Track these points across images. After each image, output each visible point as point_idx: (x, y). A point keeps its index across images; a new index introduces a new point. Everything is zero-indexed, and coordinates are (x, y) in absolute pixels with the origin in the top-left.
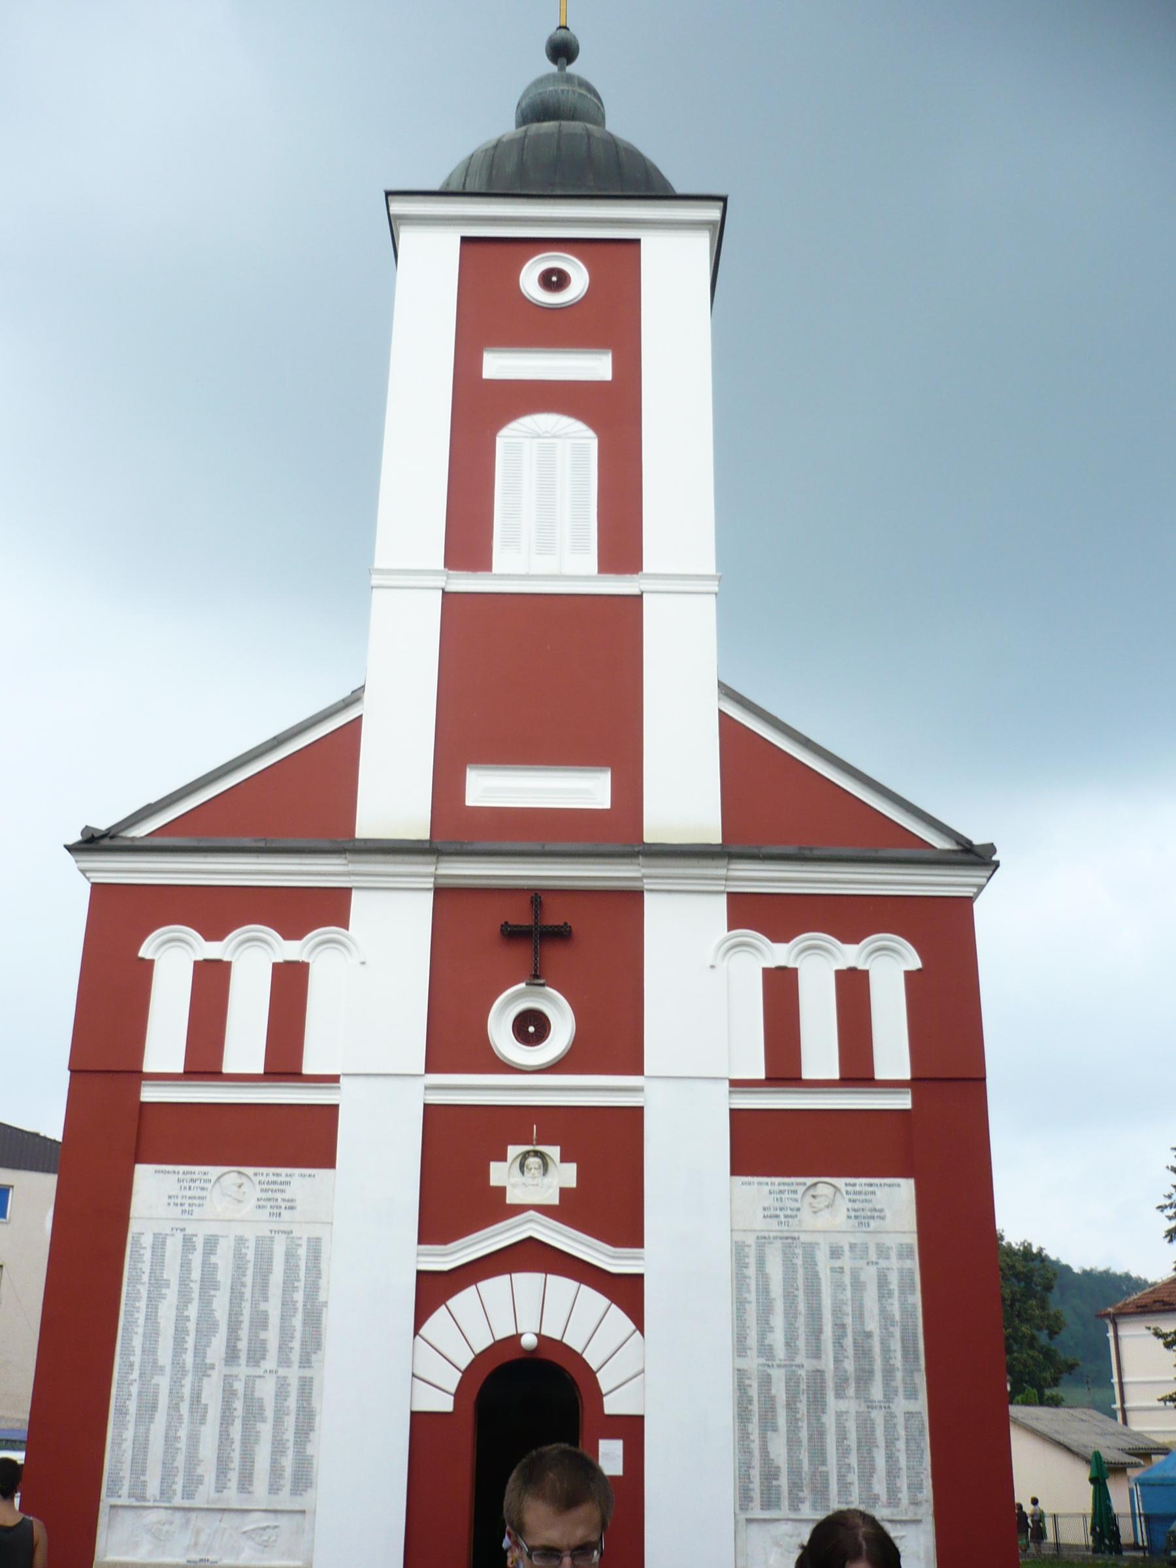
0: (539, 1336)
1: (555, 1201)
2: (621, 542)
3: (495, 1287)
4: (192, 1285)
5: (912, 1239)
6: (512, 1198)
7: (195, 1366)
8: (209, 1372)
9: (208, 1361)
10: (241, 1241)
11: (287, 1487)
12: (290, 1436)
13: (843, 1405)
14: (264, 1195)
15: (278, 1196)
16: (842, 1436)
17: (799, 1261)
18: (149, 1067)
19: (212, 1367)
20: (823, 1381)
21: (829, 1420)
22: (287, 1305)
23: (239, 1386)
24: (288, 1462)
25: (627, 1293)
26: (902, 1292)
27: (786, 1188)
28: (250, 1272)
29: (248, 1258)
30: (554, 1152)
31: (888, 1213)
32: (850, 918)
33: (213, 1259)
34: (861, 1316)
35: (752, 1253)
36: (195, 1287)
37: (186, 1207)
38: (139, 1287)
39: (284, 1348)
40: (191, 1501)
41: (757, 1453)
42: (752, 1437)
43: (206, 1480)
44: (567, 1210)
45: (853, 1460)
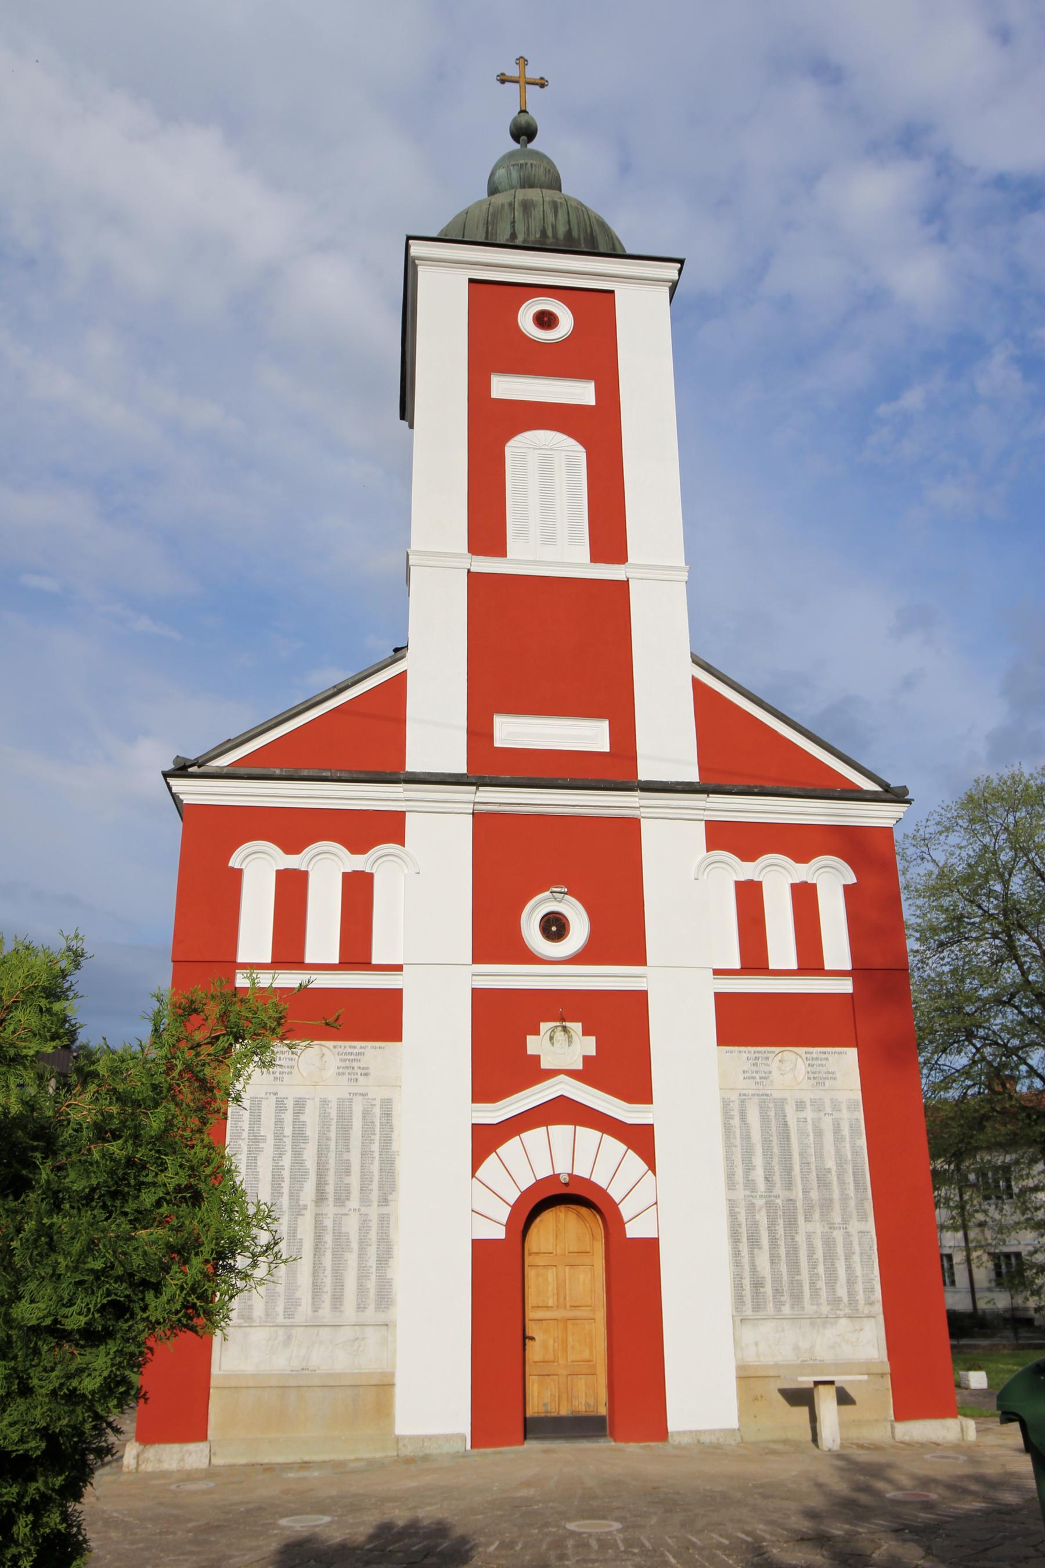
1: (579, 1066)
2: (608, 536)
3: (535, 1137)
4: (285, 1139)
5: (858, 1096)
6: (544, 1065)
7: (291, 1207)
8: (303, 1212)
9: (301, 1203)
10: (324, 1102)
11: (372, 1306)
12: (372, 1262)
13: (810, 1227)
14: (343, 1064)
15: (355, 1064)
16: (811, 1253)
17: (772, 1114)
18: (241, 959)
19: (305, 1207)
20: (795, 1208)
21: (801, 1239)
22: (365, 1154)
23: (328, 1223)
24: (372, 1284)
25: (640, 1140)
26: (852, 1137)
28: (333, 1128)
29: (331, 1116)
30: (576, 1027)
31: (838, 1075)
32: (800, 843)
33: (302, 1118)
34: (822, 1156)
35: (736, 1107)
36: (288, 1141)
37: (278, 1075)
38: (240, 1142)
39: (364, 1189)
40: (292, 1320)
41: (747, 1267)
42: (742, 1254)
43: (303, 1302)
44: (589, 1073)
45: (821, 1269)
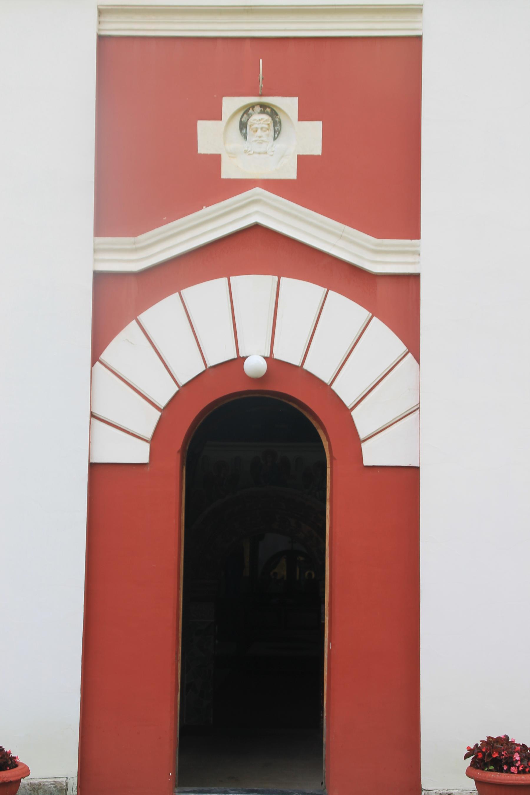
0: (270, 360)
1: (292, 174)
3: (207, 296)
6: (229, 171)
25: (396, 301)
30: (288, 105)
44: (308, 185)
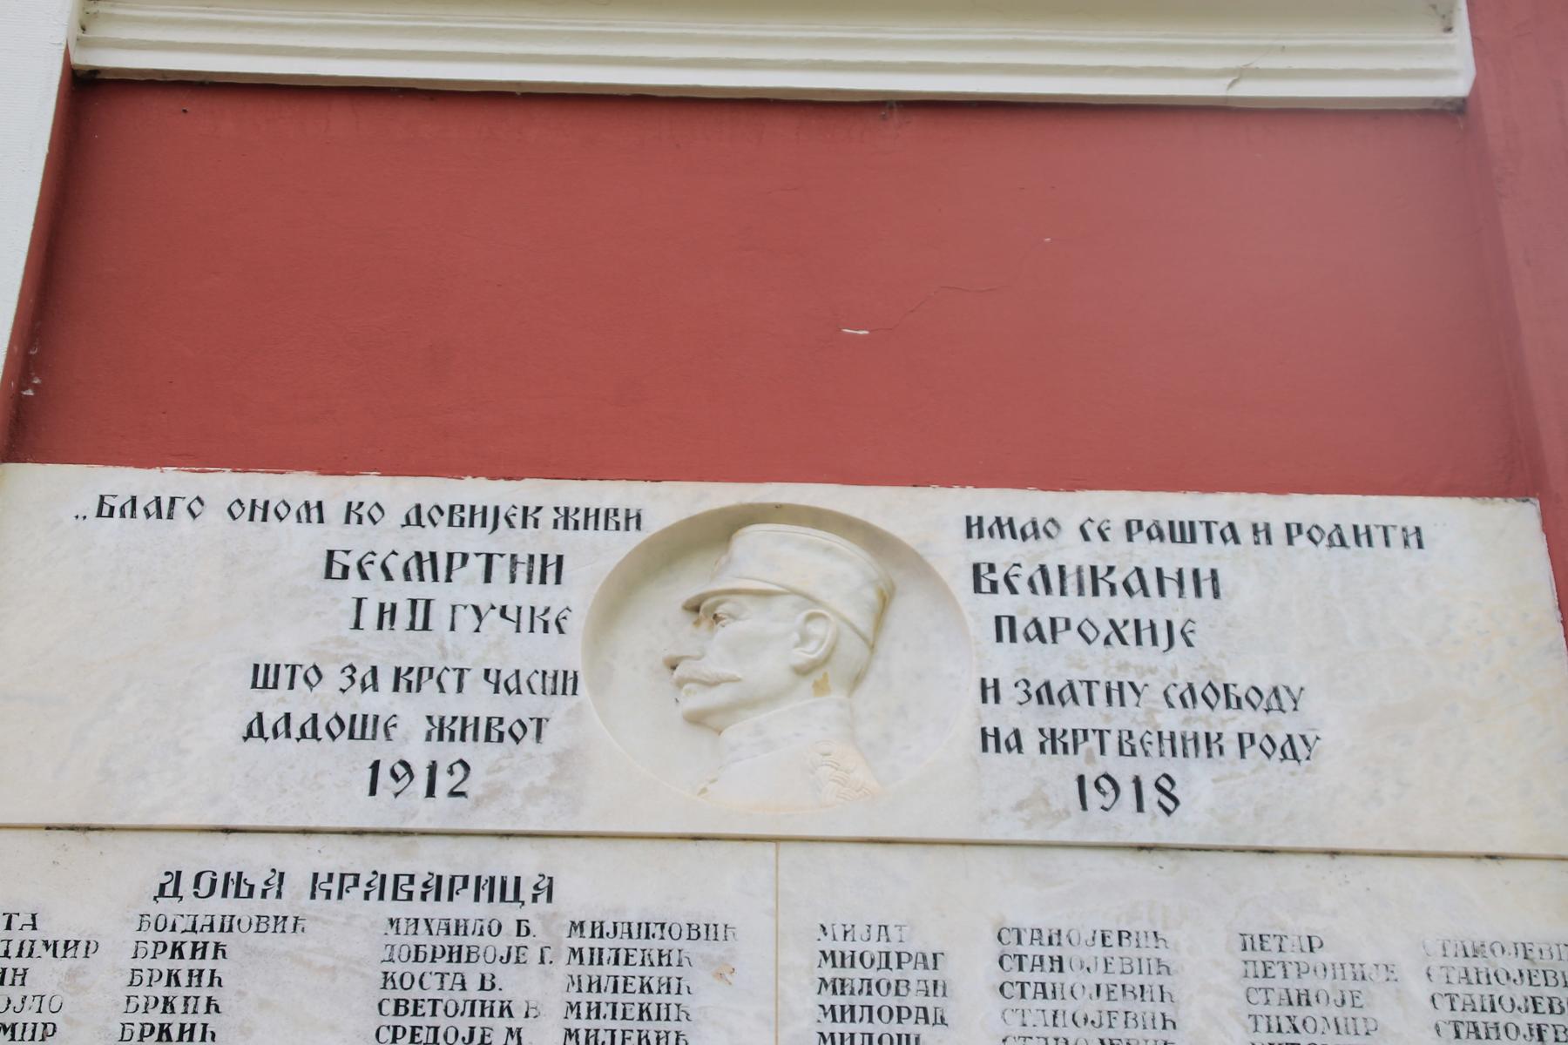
27: (474, 540)
31: (1318, 713)
